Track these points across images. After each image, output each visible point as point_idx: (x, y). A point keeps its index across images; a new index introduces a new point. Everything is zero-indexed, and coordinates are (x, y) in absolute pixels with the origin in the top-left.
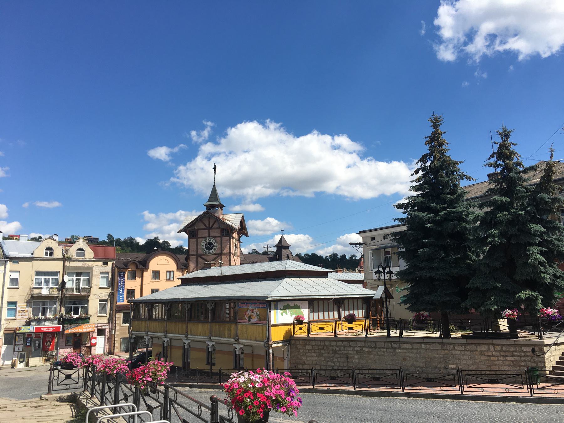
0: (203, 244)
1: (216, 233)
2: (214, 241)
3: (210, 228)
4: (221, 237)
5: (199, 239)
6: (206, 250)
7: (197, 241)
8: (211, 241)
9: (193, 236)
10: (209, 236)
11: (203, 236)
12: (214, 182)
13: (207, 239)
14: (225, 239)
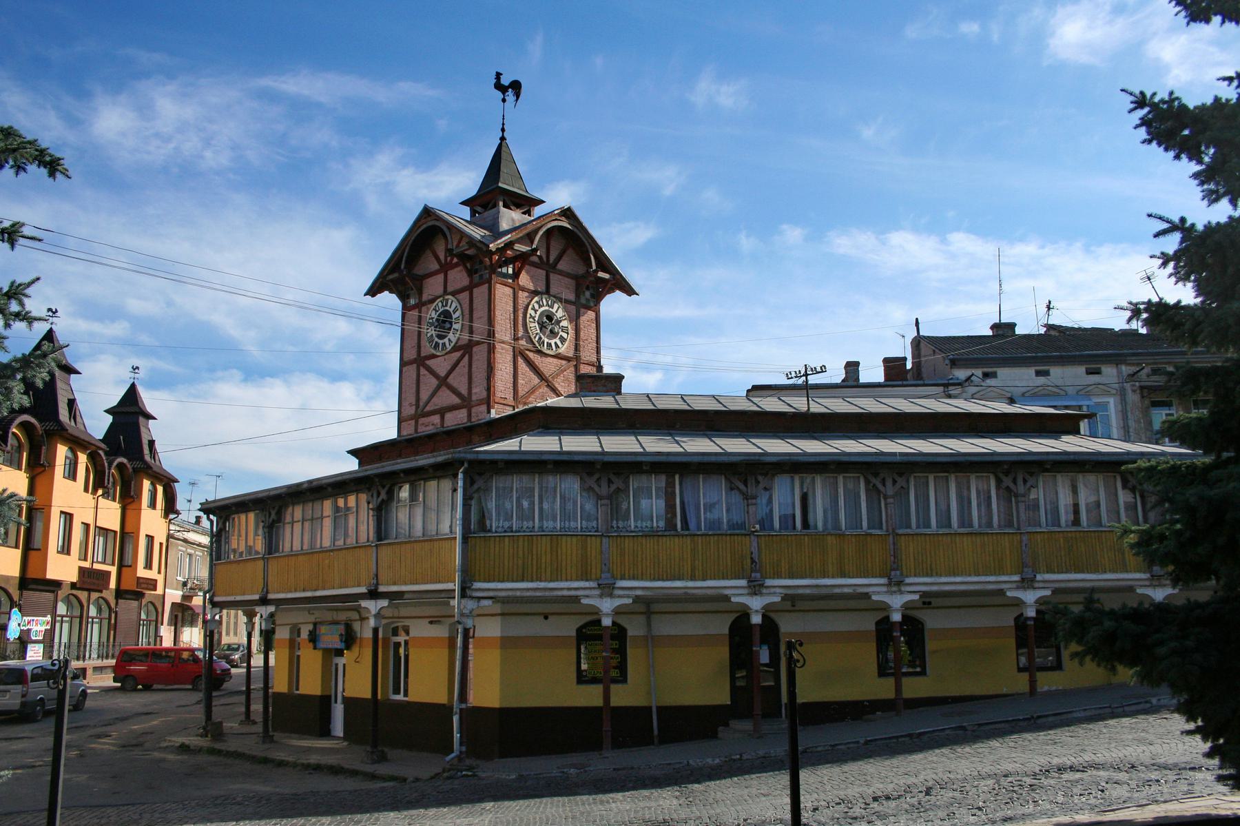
1: (459, 277)
3: (445, 268)
4: (470, 288)
6: (436, 339)
8: (448, 308)
10: (445, 292)
12: (503, 130)
13: (440, 304)
14: (480, 293)
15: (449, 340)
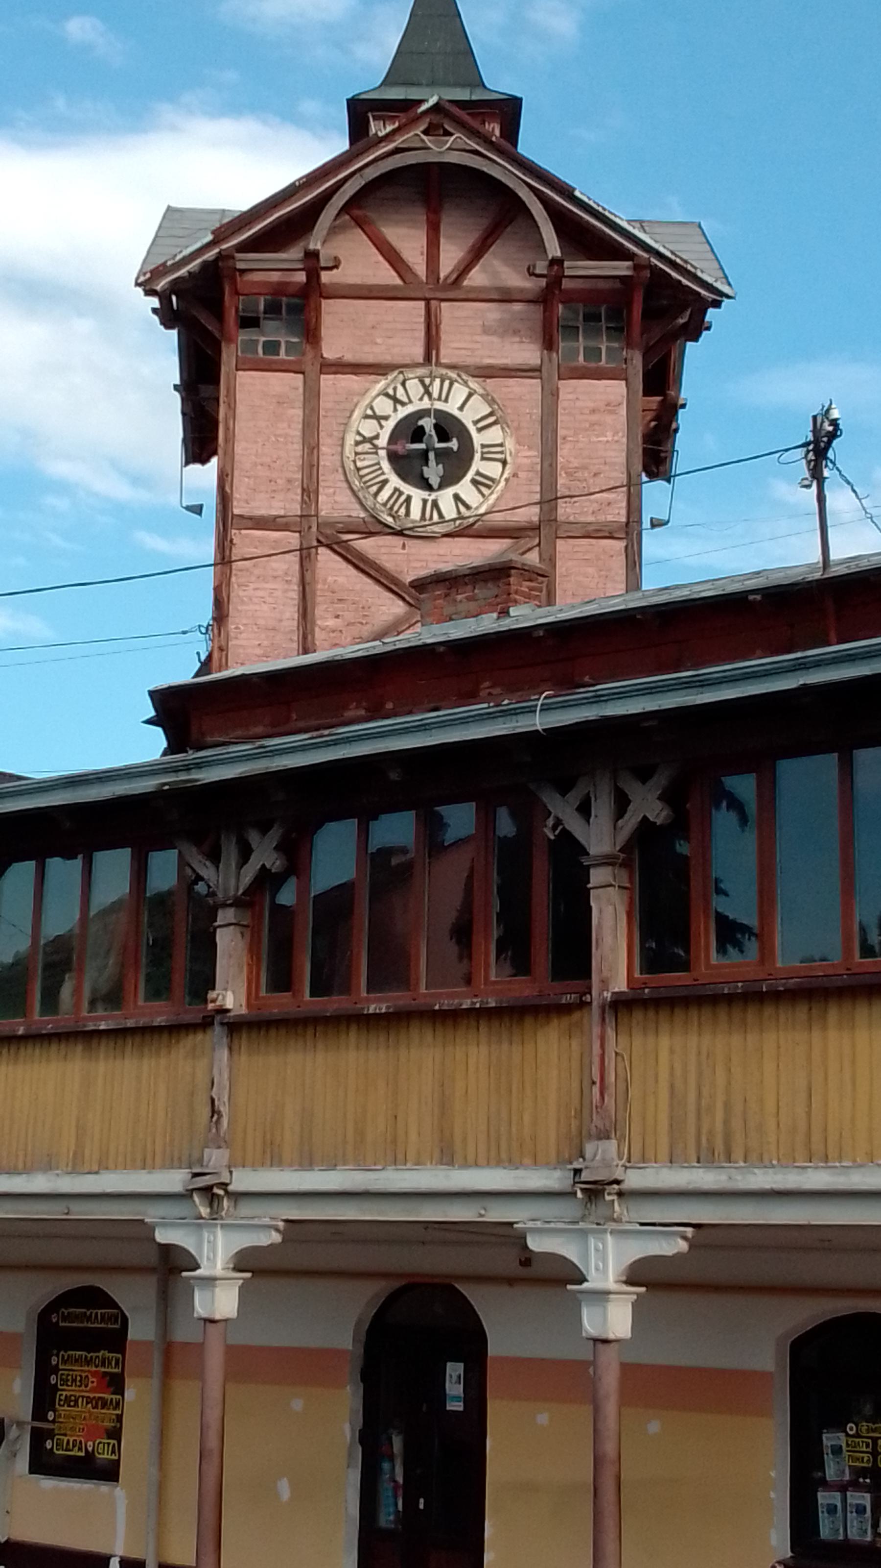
0: (368, 428)
2: (478, 408)
5: (327, 381)
6: (395, 481)
7: (312, 396)
8: (452, 407)
9: (272, 347)
11: (369, 355)
15: (457, 497)
